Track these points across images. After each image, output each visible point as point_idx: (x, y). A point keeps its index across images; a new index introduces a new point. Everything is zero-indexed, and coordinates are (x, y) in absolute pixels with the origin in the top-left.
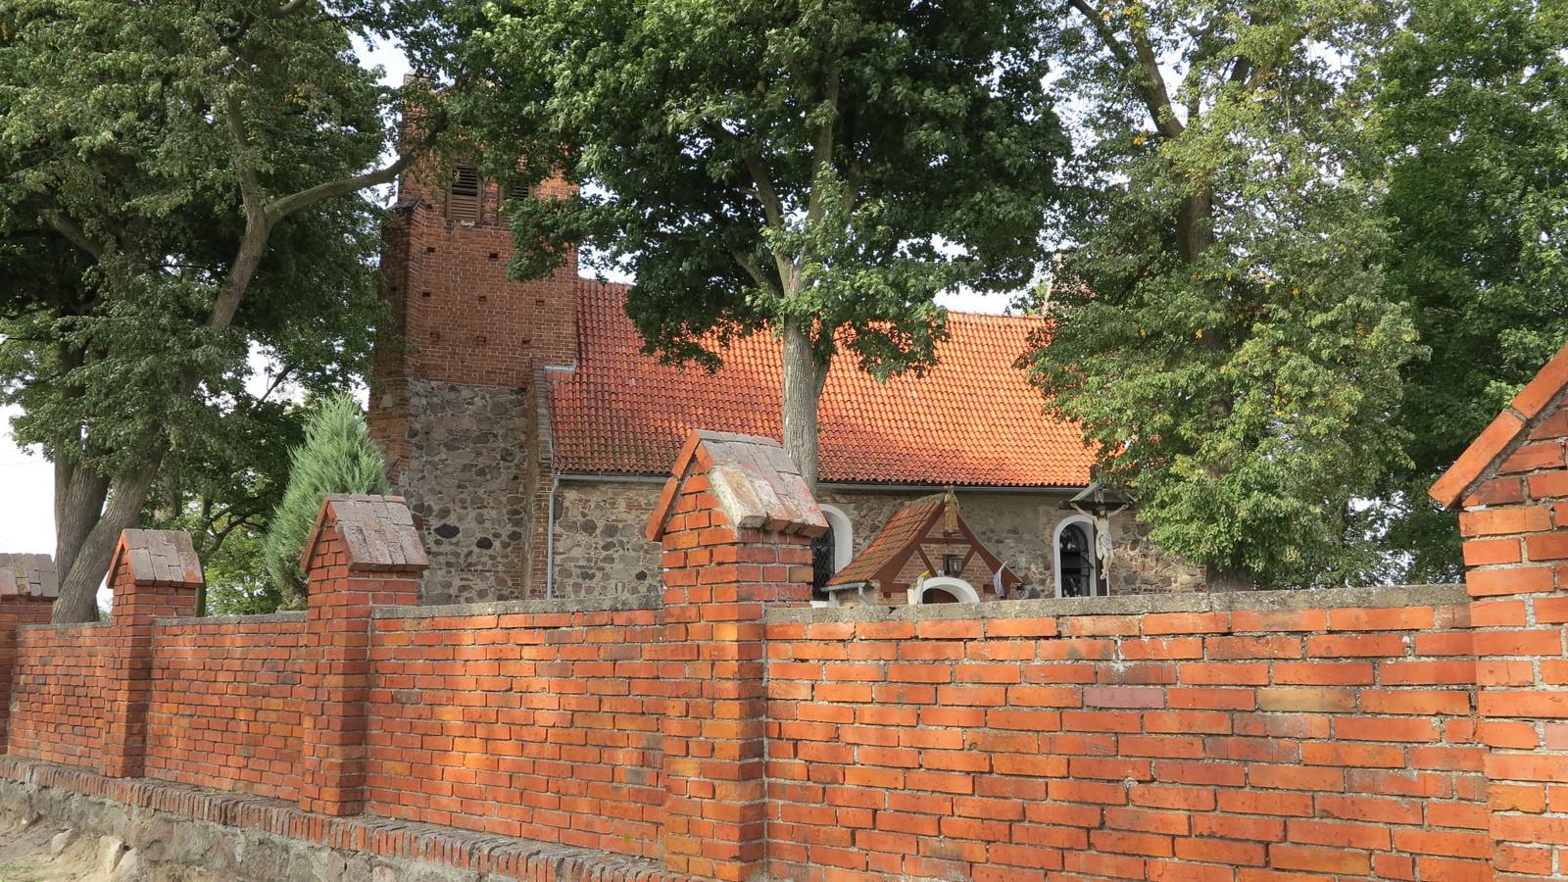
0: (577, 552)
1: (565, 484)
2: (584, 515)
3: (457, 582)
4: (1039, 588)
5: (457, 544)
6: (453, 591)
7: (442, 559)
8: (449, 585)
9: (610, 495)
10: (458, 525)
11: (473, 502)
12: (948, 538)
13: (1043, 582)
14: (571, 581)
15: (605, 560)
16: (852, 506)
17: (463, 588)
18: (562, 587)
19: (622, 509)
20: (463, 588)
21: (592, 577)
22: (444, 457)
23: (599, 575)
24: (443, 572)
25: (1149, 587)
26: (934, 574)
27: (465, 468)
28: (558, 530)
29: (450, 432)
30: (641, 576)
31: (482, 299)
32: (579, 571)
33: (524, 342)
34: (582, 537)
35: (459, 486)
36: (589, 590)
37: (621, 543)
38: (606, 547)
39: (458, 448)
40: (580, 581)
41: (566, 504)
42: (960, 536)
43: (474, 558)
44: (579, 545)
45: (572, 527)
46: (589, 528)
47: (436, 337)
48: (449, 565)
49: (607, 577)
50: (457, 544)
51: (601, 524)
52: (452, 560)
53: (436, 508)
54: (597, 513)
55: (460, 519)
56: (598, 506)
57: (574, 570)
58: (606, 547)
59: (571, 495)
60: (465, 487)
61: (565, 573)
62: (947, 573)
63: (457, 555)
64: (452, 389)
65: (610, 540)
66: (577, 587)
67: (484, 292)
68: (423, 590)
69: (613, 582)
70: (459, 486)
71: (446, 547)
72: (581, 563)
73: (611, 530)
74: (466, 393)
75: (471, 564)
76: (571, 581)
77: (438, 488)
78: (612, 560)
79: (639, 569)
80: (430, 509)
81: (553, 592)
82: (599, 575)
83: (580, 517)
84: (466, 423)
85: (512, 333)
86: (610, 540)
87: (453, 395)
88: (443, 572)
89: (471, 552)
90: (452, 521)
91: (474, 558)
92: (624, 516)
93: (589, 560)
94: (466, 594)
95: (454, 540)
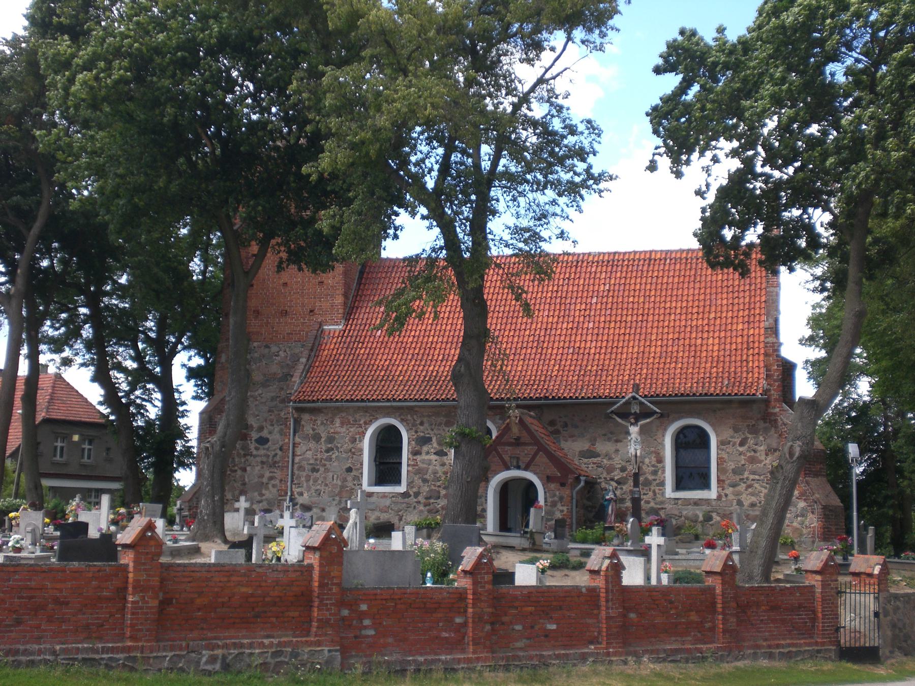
0: (309, 454)
1: (299, 410)
2: (314, 430)
3: (267, 474)
4: (651, 477)
5: (268, 449)
6: (265, 480)
7: (259, 459)
8: (262, 476)
9: (330, 415)
10: (268, 436)
11: (277, 421)
12: (518, 443)
13: (655, 473)
14: (304, 474)
15: (326, 460)
16: (498, 417)
17: (271, 478)
18: (299, 477)
19: (337, 425)
20: (271, 478)
21: (318, 471)
22: (260, 391)
23: (322, 469)
24: (259, 468)
25: (757, 477)
26: (508, 469)
27: (273, 399)
28: (297, 440)
29: (265, 375)
30: (349, 470)
31: (285, 284)
32: (310, 467)
33: (311, 311)
34: (312, 445)
35: (269, 411)
36: (316, 480)
37: (337, 448)
38: (328, 451)
39: (269, 386)
40: (310, 473)
41: (303, 423)
42: (526, 438)
43: (278, 459)
44: (310, 450)
45: (306, 438)
46: (317, 438)
47: (257, 313)
48: (263, 463)
49: (327, 470)
50: (268, 449)
51: (324, 436)
52: (264, 459)
53: (255, 425)
54: (322, 428)
55: (270, 433)
56: (322, 423)
57: (306, 466)
58: (328, 451)
59: (306, 417)
60: (273, 411)
61: (301, 468)
62: (518, 468)
63: (268, 456)
64: (267, 347)
65: (330, 446)
66: (308, 478)
67: (286, 280)
68: (247, 480)
69: (330, 474)
70: (269, 411)
71: (262, 452)
72: (312, 462)
73: (330, 440)
74: (274, 349)
75: (275, 462)
76: (304, 474)
77: (257, 413)
78: (330, 459)
79: (348, 465)
80: (252, 426)
81: (292, 481)
82: (322, 469)
83: (311, 432)
84: (275, 369)
85: (303, 305)
86: (330, 446)
87: (267, 351)
88: (259, 468)
89: (276, 454)
90: (265, 434)
91: (278, 459)
92: (339, 430)
93: (316, 460)
94: (273, 482)
95: (266, 446)
